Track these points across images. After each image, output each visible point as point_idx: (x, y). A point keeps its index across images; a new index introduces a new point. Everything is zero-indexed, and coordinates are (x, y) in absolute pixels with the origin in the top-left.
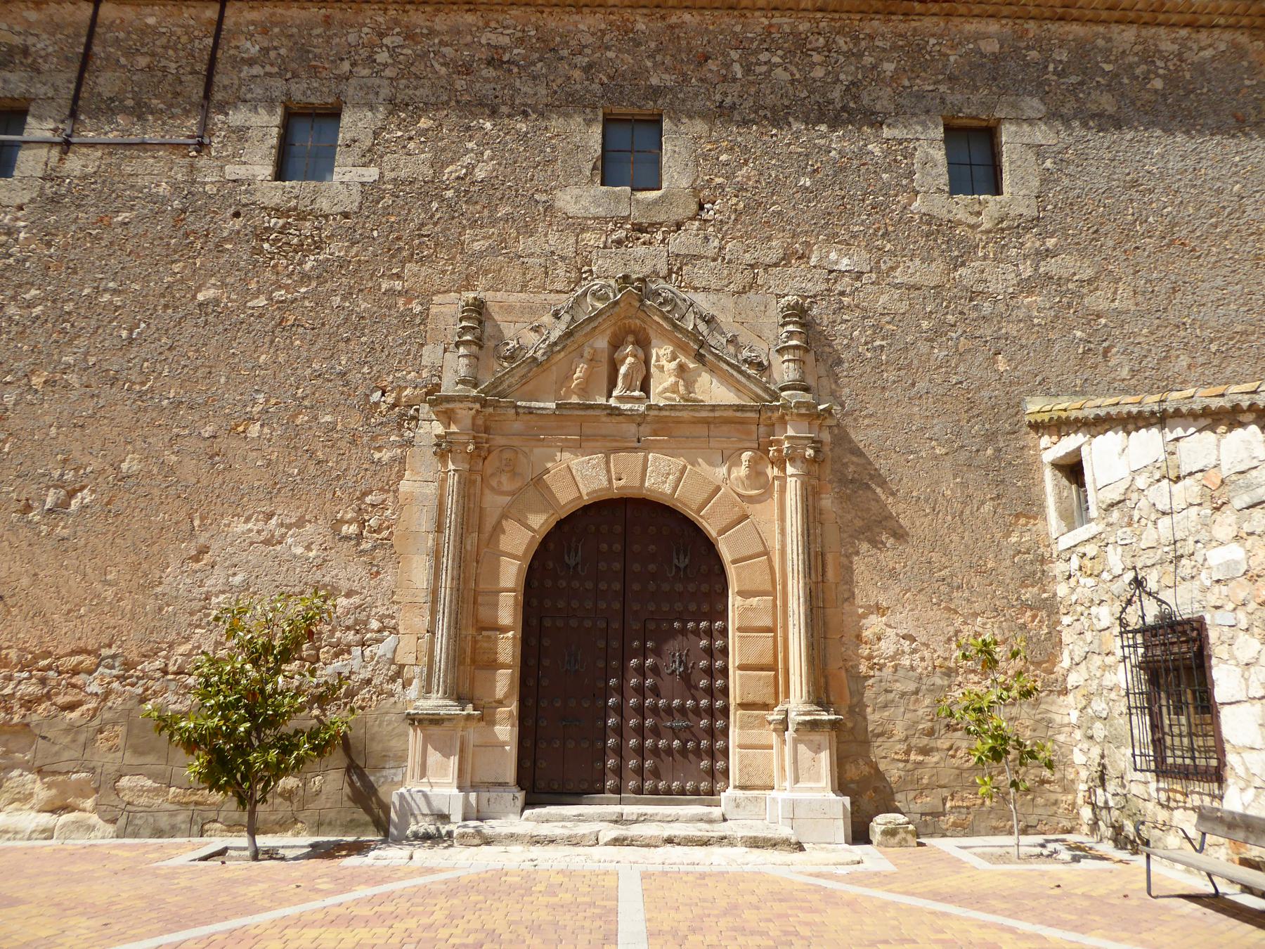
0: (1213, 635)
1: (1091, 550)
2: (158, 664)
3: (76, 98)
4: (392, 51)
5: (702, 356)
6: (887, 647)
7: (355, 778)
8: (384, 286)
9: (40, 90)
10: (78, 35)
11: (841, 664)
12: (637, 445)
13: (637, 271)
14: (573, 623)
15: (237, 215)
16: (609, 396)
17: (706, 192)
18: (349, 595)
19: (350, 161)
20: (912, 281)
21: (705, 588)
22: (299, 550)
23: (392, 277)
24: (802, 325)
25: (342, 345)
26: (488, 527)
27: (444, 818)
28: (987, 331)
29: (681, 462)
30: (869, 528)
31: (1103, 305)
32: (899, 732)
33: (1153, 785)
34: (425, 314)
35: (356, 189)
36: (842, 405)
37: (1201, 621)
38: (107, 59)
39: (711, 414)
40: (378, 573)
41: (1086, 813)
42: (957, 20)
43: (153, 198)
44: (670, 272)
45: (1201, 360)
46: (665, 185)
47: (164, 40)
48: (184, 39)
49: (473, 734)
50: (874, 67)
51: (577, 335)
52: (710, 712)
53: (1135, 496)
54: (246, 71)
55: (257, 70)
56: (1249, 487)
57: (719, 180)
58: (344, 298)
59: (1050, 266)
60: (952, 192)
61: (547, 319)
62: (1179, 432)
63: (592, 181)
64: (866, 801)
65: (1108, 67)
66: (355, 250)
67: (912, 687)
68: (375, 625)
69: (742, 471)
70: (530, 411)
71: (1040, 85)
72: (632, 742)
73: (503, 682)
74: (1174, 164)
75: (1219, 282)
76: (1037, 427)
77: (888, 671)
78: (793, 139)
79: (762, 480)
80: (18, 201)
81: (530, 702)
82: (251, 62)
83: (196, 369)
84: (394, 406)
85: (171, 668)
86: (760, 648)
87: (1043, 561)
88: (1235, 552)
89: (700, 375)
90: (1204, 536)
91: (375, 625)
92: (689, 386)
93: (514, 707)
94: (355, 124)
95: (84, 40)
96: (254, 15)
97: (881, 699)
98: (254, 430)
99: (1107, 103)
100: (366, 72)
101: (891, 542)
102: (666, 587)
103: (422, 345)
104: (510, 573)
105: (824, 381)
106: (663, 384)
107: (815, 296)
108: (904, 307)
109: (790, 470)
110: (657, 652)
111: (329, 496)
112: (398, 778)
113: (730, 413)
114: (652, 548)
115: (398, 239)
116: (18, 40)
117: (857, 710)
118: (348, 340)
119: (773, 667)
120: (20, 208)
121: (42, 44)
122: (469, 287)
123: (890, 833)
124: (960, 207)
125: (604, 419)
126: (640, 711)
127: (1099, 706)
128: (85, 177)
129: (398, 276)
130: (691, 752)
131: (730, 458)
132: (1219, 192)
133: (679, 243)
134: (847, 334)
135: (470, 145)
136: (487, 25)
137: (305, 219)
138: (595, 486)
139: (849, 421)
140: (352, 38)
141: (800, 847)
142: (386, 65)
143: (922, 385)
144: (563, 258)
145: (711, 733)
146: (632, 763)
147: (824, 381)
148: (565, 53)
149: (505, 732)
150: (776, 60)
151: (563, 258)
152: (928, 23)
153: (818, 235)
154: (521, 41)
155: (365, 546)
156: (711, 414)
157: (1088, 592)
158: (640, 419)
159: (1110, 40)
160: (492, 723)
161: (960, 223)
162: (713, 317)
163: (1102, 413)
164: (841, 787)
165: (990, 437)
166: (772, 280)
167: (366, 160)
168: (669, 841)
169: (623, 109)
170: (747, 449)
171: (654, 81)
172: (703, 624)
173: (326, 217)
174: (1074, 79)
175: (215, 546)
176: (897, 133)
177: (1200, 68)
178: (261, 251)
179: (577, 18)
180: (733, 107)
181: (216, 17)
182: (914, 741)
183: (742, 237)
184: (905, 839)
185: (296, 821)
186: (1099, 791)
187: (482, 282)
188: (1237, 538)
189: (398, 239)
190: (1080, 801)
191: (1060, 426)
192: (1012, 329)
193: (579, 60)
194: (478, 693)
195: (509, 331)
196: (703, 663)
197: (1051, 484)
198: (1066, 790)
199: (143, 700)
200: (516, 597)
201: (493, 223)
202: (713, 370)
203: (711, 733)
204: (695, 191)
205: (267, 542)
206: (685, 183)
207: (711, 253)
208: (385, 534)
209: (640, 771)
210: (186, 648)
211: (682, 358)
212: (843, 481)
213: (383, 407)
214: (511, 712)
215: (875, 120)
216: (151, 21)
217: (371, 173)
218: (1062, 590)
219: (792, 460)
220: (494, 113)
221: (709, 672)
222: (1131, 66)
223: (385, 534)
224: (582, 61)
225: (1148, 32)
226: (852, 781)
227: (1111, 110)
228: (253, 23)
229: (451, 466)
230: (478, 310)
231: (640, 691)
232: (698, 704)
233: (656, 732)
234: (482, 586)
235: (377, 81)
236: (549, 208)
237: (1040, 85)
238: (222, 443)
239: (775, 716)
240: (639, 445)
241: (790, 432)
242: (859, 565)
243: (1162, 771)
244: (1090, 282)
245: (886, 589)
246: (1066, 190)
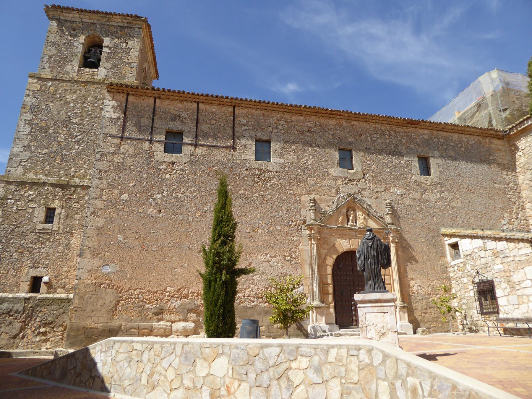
0: (495, 283)
1: (461, 265)
2: (242, 294)
3: (196, 132)
4: (282, 125)
6: (415, 288)
8: (289, 192)
9: (186, 128)
10: (194, 113)
13: (352, 192)
15: (247, 170)
19: (275, 156)
20: (414, 197)
22: (276, 264)
24: (391, 208)
25: (280, 208)
27: (324, 332)
28: (431, 211)
31: (455, 205)
32: (419, 309)
33: (480, 317)
34: (300, 200)
35: (278, 165)
37: (492, 281)
38: (203, 120)
41: (461, 327)
42: (418, 129)
43: (223, 163)
45: (476, 219)
47: (218, 116)
48: (224, 116)
50: (401, 141)
53: (474, 253)
54: (243, 128)
55: (246, 128)
56: (504, 253)
58: (279, 195)
59: (443, 195)
60: (421, 175)
61: (331, 203)
62: (486, 241)
64: (416, 325)
65: (452, 144)
66: (280, 182)
67: (421, 298)
70: (331, 228)
71: (438, 148)
73: (331, 298)
74: (468, 170)
75: (479, 200)
76: (444, 235)
77: (416, 294)
78: (383, 159)
80: (184, 162)
81: (337, 304)
82: (244, 125)
83: (242, 213)
85: (246, 296)
87: (447, 268)
88: (501, 266)
90: (493, 263)
92: (367, 222)
93: (333, 304)
94: (275, 146)
95: (196, 114)
96: (243, 111)
98: (260, 231)
99: (452, 153)
100: (276, 131)
101: (414, 263)
104: (329, 270)
105: (397, 222)
106: (360, 221)
108: (412, 204)
112: (308, 323)
115: (291, 179)
116: (177, 113)
117: (410, 303)
118: (281, 207)
120: (185, 164)
121: (183, 114)
122: (310, 194)
124: (423, 179)
127: (464, 301)
128: (202, 156)
129: (292, 190)
132: (478, 178)
133: (360, 184)
134: (401, 210)
135: (306, 154)
136: (306, 120)
137: (265, 172)
138: (347, 248)
139: (403, 232)
140: (271, 121)
141: (406, 334)
142: (281, 130)
143: (418, 224)
148: (327, 130)
149: (332, 310)
150: (378, 137)
151: (333, 187)
152: (412, 129)
154: (315, 126)
157: (460, 275)
158: (356, 231)
159: (452, 137)
161: (423, 183)
163: (466, 234)
165: (434, 237)
167: (280, 156)
169: (343, 147)
171: (350, 140)
173: (271, 172)
174: (445, 147)
175: (254, 262)
176: (408, 159)
177: (472, 146)
178: (254, 180)
179: (329, 120)
180: (369, 149)
181: (232, 111)
182: (423, 311)
185: (283, 335)
186: (465, 321)
187: (313, 192)
188: (501, 263)
189: (291, 179)
190: (458, 324)
191: (451, 236)
192: (436, 210)
193: (330, 132)
194: (325, 300)
195: (322, 206)
197: (448, 250)
198: (455, 322)
199: (240, 304)
204: (363, 171)
205: (267, 261)
206: (360, 169)
207: (368, 188)
208: (297, 259)
210: (248, 290)
212: (403, 248)
213: (293, 226)
215: (402, 155)
216: (214, 110)
217: (282, 161)
218: (452, 274)
219: (392, 242)
220: (311, 146)
222: (457, 144)
223: (297, 259)
224: (332, 133)
225: (461, 135)
227: (453, 155)
228: (243, 113)
229: (313, 242)
230: (314, 200)
234: (323, 273)
235: (280, 134)
237: (438, 148)
238: (252, 234)
241: (391, 235)
242: (408, 268)
243: (482, 313)
244: (452, 199)
245: (414, 274)
246: (445, 176)
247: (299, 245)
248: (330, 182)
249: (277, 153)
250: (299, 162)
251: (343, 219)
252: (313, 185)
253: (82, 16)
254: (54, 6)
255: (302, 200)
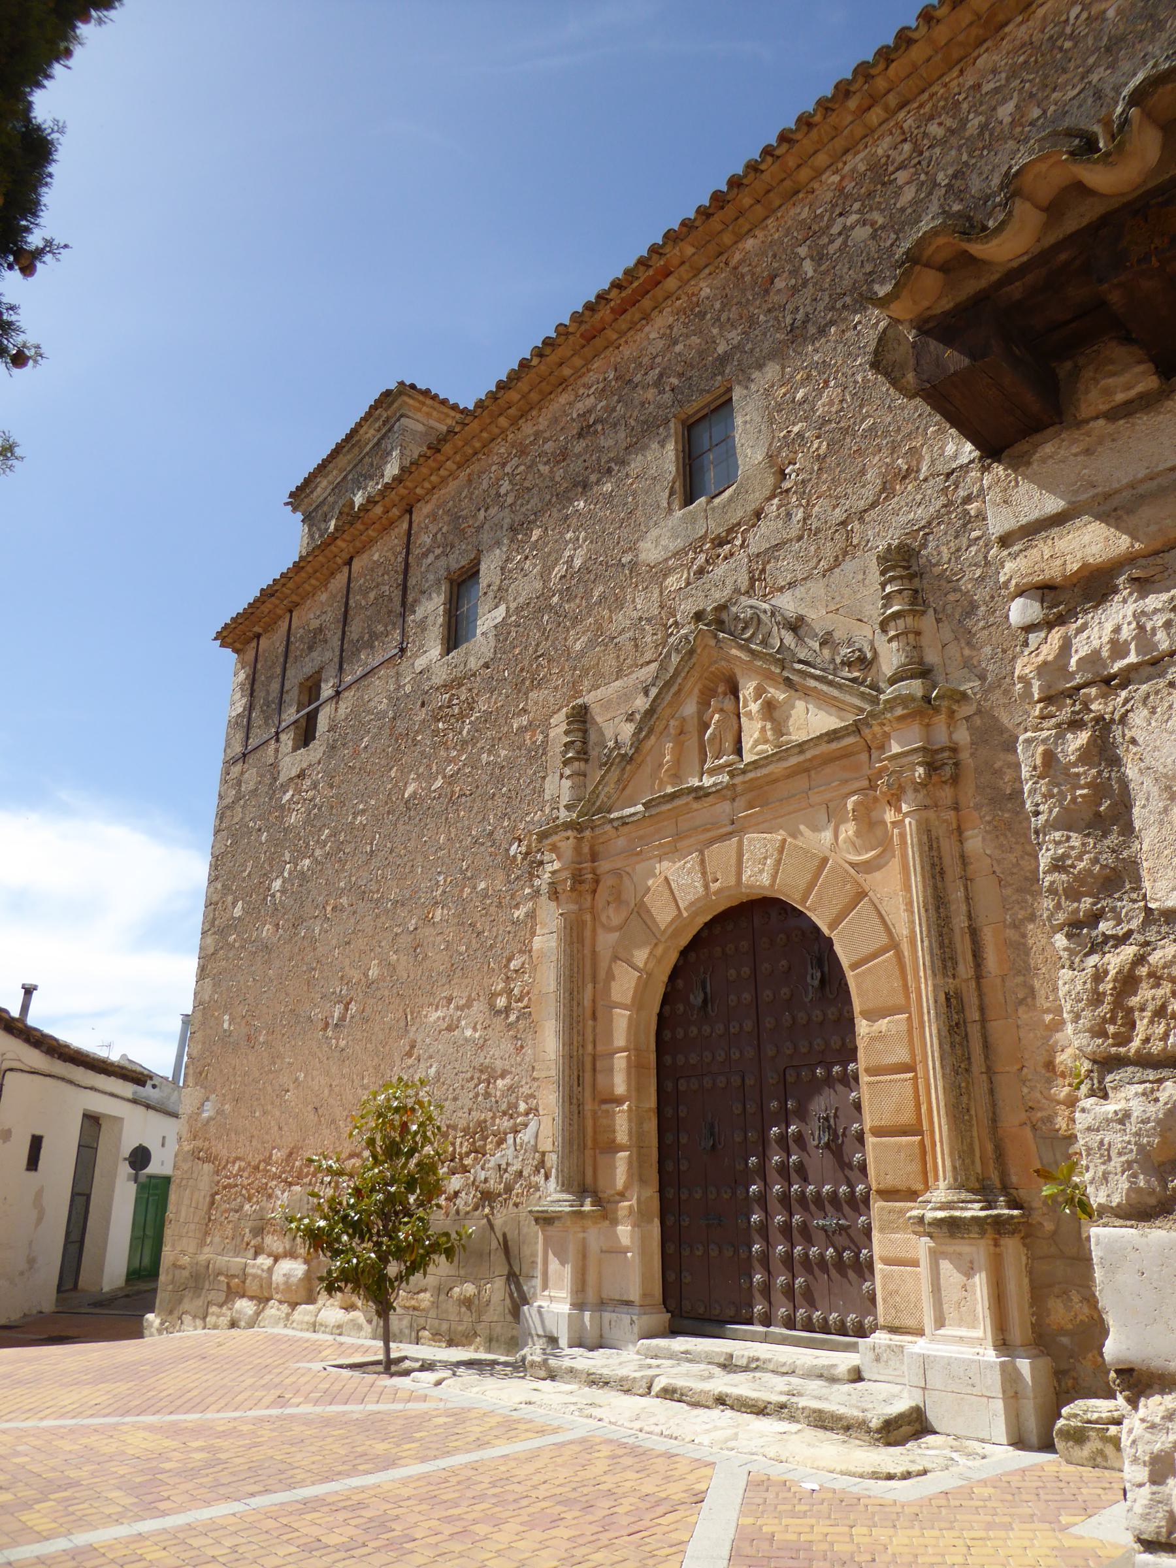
5: (787, 680)
7: (513, 1287)
11: (1023, 1116)
12: (729, 829)
14: (707, 1082)
18: (503, 1076)
26: (602, 974)
29: (778, 836)
36: (982, 678)
39: (801, 758)
40: (522, 1047)
44: (752, 580)
49: (594, 1236)
51: (659, 710)
57: (796, 429)
63: (670, 510)
68: (522, 1107)
79: (879, 832)
89: (793, 707)
91: (522, 1107)
103: (544, 778)
105: (953, 650)
107: (929, 523)
110: (802, 1114)
113: (825, 748)
115: (522, 670)
125: (695, 805)
130: (849, 1267)
147: (953, 650)
151: (649, 620)
153: (926, 429)
156: (801, 758)
160: (615, 1222)
162: (801, 619)
170: (854, 793)
183: (829, 489)
184: (1101, 1452)
185: (476, 1335)
189: (522, 670)
200: (628, 1057)
202: (807, 693)
206: (759, 456)
209: (789, 1291)
214: (631, 1207)
226: (1062, 1331)
232: (853, 1192)
240: (736, 829)
247: (533, 934)
252: (583, 653)
253: (330, 478)
254: (292, 495)
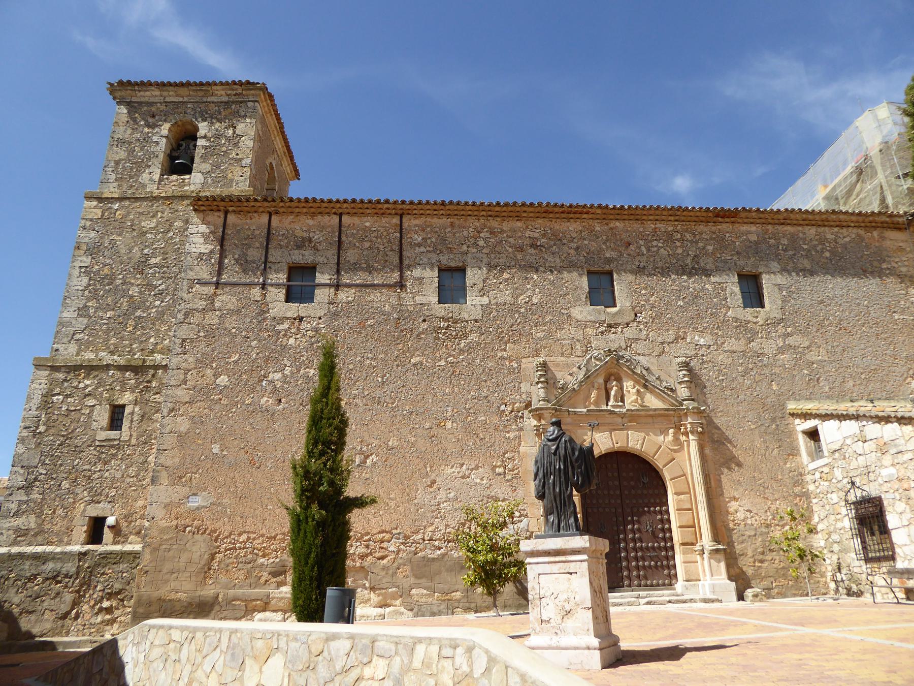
0: (885, 503)
1: (826, 470)
2: (420, 536)
3: (338, 264)
4: (485, 239)
8: (499, 355)
9: (320, 259)
10: (333, 232)
13: (614, 346)
15: (424, 321)
16: (607, 405)
17: (638, 308)
18: (503, 500)
19: (474, 294)
20: (732, 349)
21: (656, 492)
22: (478, 481)
23: (502, 350)
24: (688, 371)
25: (483, 383)
28: (767, 371)
29: (643, 434)
30: (727, 462)
31: (815, 358)
32: (750, 553)
33: (864, 567)
34: (519, 367)
35: (479, 308)
37: (880, 498)
38: (350, 243)
41: (832, 585)
42: (737, 225)
43: (383, 313)
45: (858, 382)
46: (618, 305)
48: (385, 234)
50: (704, 248)
52: (666, 548)
53: (846, 447)
55: (422, 249)
56: (896, 446)
58: (481, 361)
59: (790, 341)
60: (745, 307)
61: (575, 369)
62: (864, 423)
64: (742, 585)
65: (805, 247)
66: (482, 338)
67: (753, 533)
69: (670, 437)
70: (575, 413)
71: (777, 256)
72: (633, 563)
74: (838, 292)
75: (862, 346)
76: (792, 415)
77: (742, 526)
78: (673, 282)
80: (319, 315)
82: (419, 245)
83: (417, 396)
84: (512, 412)
85: (426, 538)
86: (687, 518)
87: (801, 475)
88: (892, 470)
90: (879, 464)
91: (517, 514)
92: (642, 399)
94: (473, 276)
95: (337, 234)
96: (417, 222)
97: (740, 539)
99: (806, 264)
100: (475, 250)
102: (639, 492)
105: (700, 396)
108: (730, 361)
109: (691, 437)
111: (488, 455)
113: (662, 412)
114: (631, 474)
115: (502, 332)
116: (305, 235)
117: (730, 544)
118: (486, 381)
119: (694, 526)
120: (320, 318)
121: (317, 236)
122: (537, 355)
123: (756, 596)
124: (749, 314)
126: (635, 549)
127: (835, 537)
128: (349, 303)
129: (505, 350)
131: (664, 432)
132: (859, 304)
133: (630, 332)
134: (707, 374)
135: (529, 286)
138: (607, 447)
139: (712, 414)
140: (465, 233)
141: (721, 601)
143: (742, 397)
144: (578, 341)
145: (667, 558)
146: (635, 573)
148: (565, 241)
150: (660, 245)
151: (578, 341)
152: (724, 226)
154: (544, 236)
155: (508, 477)
157: (825, 488)
158: (623, 416)
159: (805, 234)
161: (749, 321)
163: (829, 412)
164: (730, 578)
165: (773, 420)
166: (671, 349)
168: (670, 602)
171: (608, 255)
172: (658, 508)
173: (467, 321)
174: (791, 253)
175: (439, 480)
177: (845, 246)
178: (437, 338)
180: (644, 268)
181: (398, 222)
182: (756, 557)
186: (838, 574)
187: (543, 352)
188: (893, 465)
189: (502, 332)
190: (828, 580)
191: (806, 416)
192: (776, 370)
193: (572, 245)
195: (559, 375)
196: (660, 526)
197: (802, 442)
198: (822, 576)
199: (416, 554)
201: (545, 324)
202: (652, 392)
203: (667, 558)
204: (633, 308)
205: (463, 477)
206: (628, 304)
207: (644, 337)
208: (516, 472)
209: (638, 577)
210: (431, 529)
211: (637, 387)
212: (713, 441)
213: (507, 412)
216: (367, 224)
217: (485, 300)
218: (811, 487)
219: (692, 433)
220: (537, 271)
221: (663, 530)
222: (815, 246)
223: (516, 472)
224: (574, 245)
225: (822, 229)
227: (808, 267)
228: (417, 225)
230: (544, 366)
231: (634, 540)
233: (643, 559)
235: (481, 255)
236: (569, 317)
237: (777, 256)
238: (435, 431)
239: (698, 547)
240: (624, 428)
241: (690, 420)
242: (724, 479)
243: (868, 560)
244: (808, 348)
246: (793, 305)
247: (520, 445)
248: (573, 331)
249: (476, 288)
250: (516, 300)
251: (598, 397)
252: (541, 339)
253: (165, 93)
254: (121, 83)
255: (523, 366)
